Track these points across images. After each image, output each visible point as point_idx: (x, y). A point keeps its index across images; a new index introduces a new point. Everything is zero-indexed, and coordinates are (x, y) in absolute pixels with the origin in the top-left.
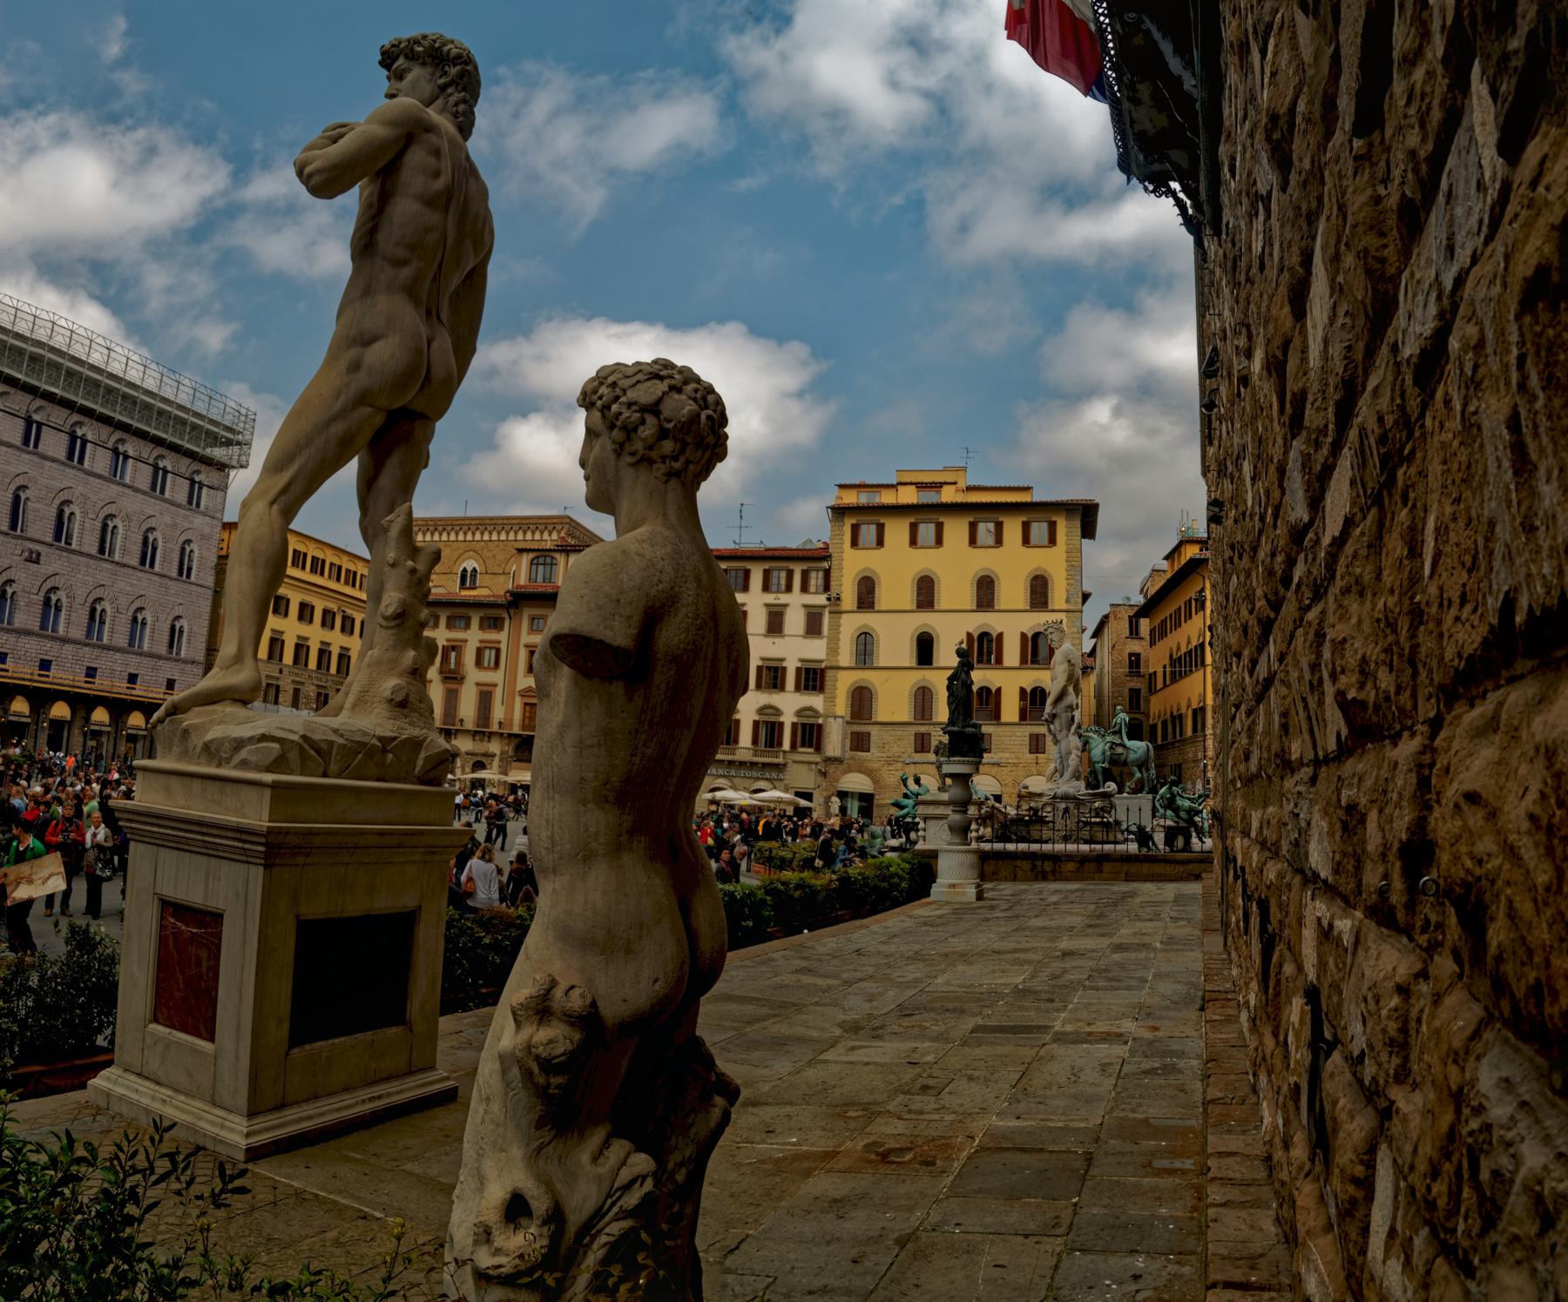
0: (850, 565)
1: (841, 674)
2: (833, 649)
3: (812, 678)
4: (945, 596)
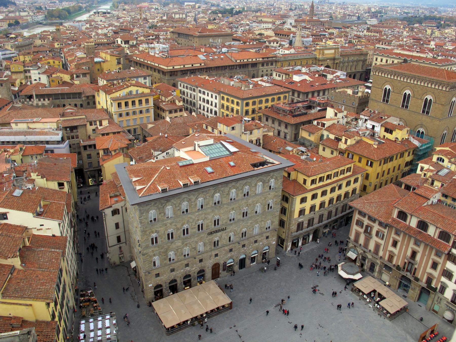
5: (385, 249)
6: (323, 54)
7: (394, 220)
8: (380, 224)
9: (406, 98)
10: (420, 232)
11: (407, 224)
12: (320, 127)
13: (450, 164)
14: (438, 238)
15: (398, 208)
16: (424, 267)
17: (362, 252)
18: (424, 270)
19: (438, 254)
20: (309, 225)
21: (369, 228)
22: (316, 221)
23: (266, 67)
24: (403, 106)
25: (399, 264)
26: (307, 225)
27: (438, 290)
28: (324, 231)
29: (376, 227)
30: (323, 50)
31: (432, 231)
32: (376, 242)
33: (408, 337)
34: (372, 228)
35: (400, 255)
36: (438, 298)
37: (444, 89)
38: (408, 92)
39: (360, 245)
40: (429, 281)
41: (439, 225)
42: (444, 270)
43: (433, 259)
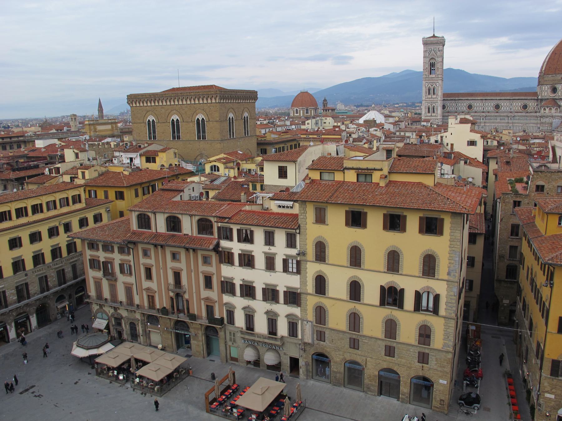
0: (312, 232)
1: (309, 297)
2: (303, 282)
3: (293, 298)
4: (368, 258)
5: (140, 290)
6: (95, 131)
7: (134, 233)
8: (121, 251)
9: (176, 126)
10: (173, 236)
11: (154, 231)
12: (54, 175)
13: (227, 170)
14: (199, 234)
15: (135, 211)
16: (196, 292)
17: (112, 311)
18: (198, 297)
19: (206, 261)
20: (20, 298)
21: (109, 265)
22: (34, 288)
23: (11, 151)
24: (174, 138)
25: (165, 306)
26: (15, 298)
27: (225, 322)
28: (59, 307)
29: (117, 258)
30: (93, 124)
31: (188, 226)
32: (124, 283)
33: (191, 409)
34: (112, 264)
35: (160, 289)
36: (230, 333)
37: (214, 101)
38: (175, 117)
39: (106, 299)
40: (210, 310)
41: (194, 212)
42: (222, 282)
43: (203, 273)
